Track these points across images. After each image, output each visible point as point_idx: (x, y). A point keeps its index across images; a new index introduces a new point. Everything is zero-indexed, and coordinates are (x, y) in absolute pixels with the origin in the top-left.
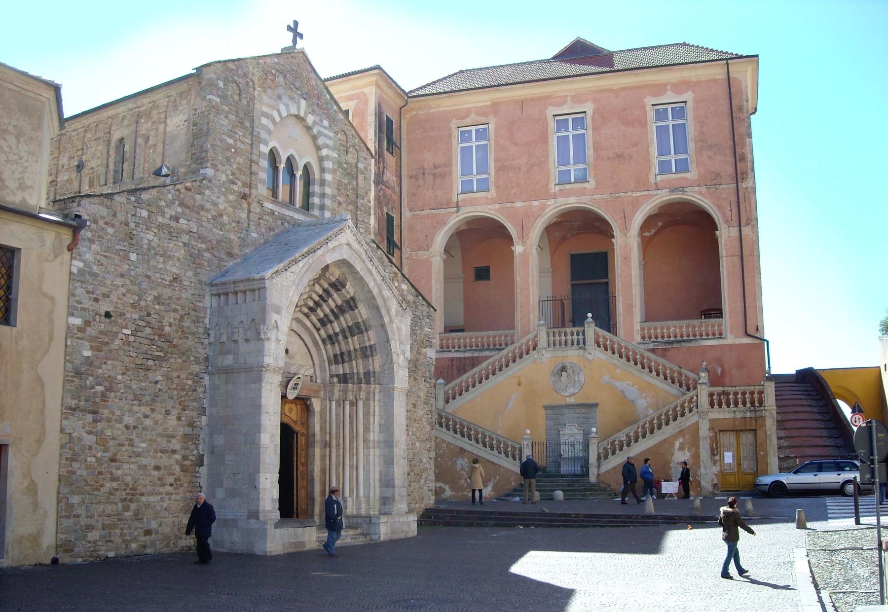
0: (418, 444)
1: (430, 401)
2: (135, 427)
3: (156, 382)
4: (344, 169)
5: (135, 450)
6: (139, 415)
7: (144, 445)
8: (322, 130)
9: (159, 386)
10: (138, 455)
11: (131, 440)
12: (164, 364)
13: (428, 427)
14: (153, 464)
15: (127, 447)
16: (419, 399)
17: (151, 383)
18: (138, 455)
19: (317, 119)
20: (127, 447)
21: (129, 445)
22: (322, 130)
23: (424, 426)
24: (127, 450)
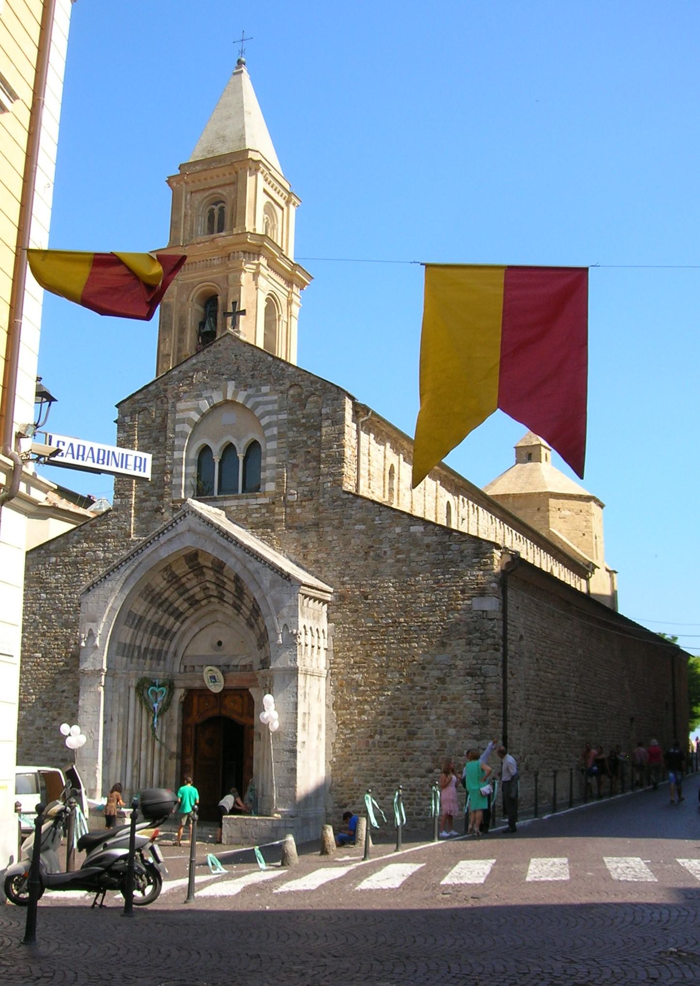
0: (451, 731)
1: (480, 669)
2: (44, 728)
3: (63, 691)
4: (303, 425)
5: (45, 745)
6: (47, 719)
7: (52, 742)
8: (260, 399)
9: (65, 694)
10: (48, 750)
11: (41, 738)
12: (70, 676)
13: (479, 706)
14: (60, 757)
15: (38, 744)
16: (454, 671)
17: (57, 692)
18: (48, 750)
19: (250, 391)
20: (38, 744)
21: (40, 742)
22: (260, 399)
23: (465, 707)
24: (38, 746)
